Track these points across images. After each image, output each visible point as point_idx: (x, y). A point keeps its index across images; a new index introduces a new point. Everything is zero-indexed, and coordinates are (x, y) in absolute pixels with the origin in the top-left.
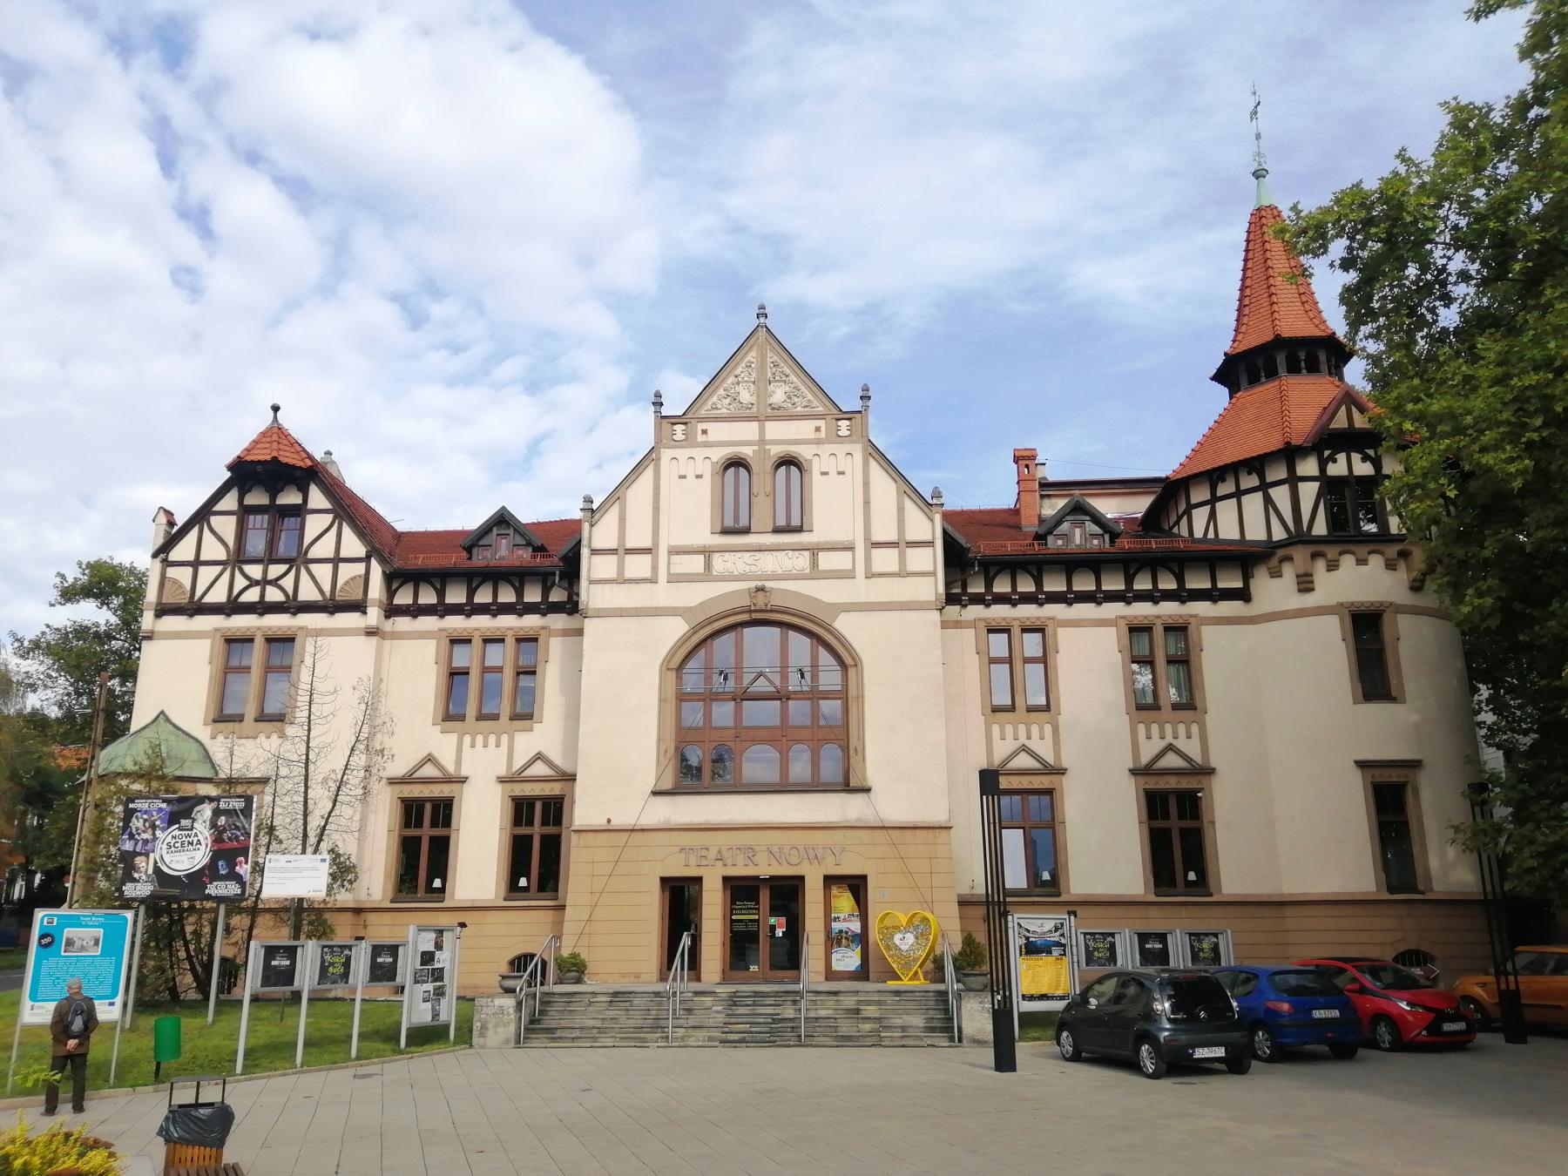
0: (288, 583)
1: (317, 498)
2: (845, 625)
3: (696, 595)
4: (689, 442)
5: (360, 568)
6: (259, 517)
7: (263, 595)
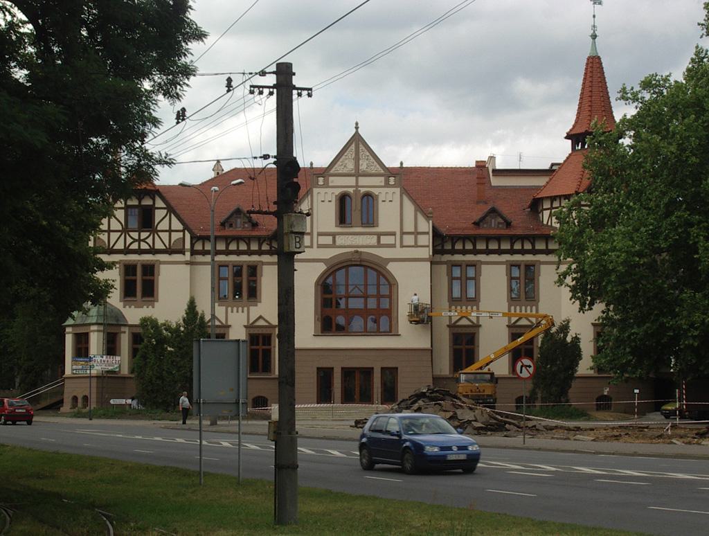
0: (150, 240)
1: (159, 203)
2: (391, 267)
3: (329, 254)
4: (326, 185)
5: (181, 235)
6: (133, 210)
7: (139, 246)
